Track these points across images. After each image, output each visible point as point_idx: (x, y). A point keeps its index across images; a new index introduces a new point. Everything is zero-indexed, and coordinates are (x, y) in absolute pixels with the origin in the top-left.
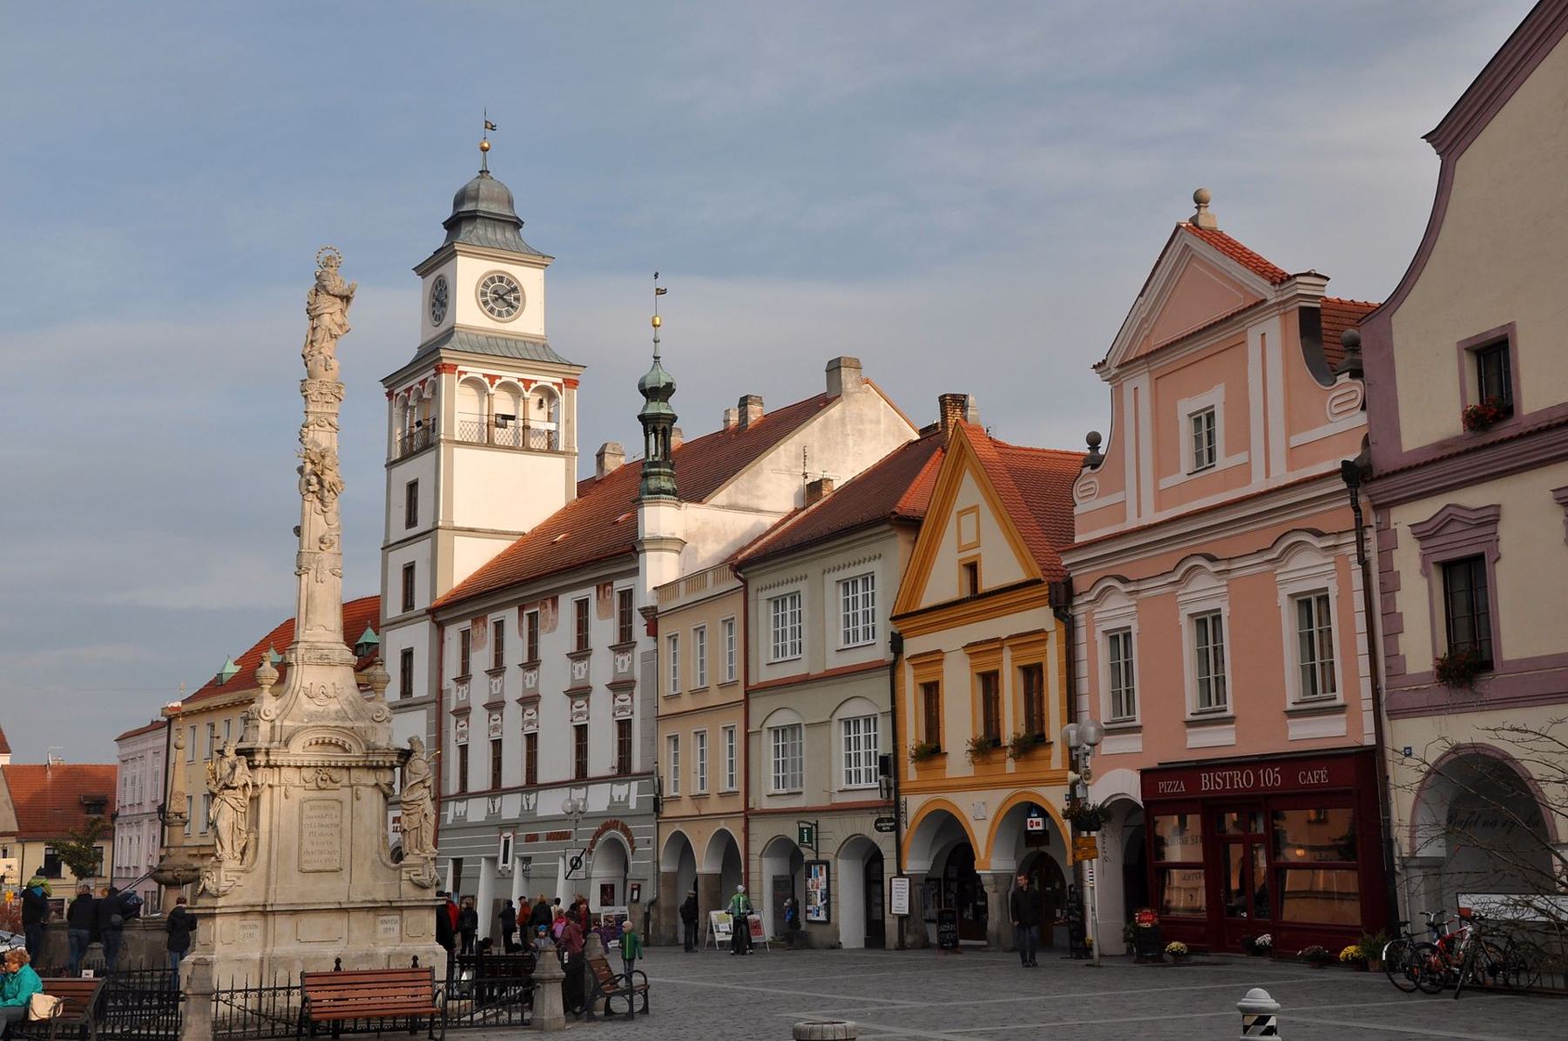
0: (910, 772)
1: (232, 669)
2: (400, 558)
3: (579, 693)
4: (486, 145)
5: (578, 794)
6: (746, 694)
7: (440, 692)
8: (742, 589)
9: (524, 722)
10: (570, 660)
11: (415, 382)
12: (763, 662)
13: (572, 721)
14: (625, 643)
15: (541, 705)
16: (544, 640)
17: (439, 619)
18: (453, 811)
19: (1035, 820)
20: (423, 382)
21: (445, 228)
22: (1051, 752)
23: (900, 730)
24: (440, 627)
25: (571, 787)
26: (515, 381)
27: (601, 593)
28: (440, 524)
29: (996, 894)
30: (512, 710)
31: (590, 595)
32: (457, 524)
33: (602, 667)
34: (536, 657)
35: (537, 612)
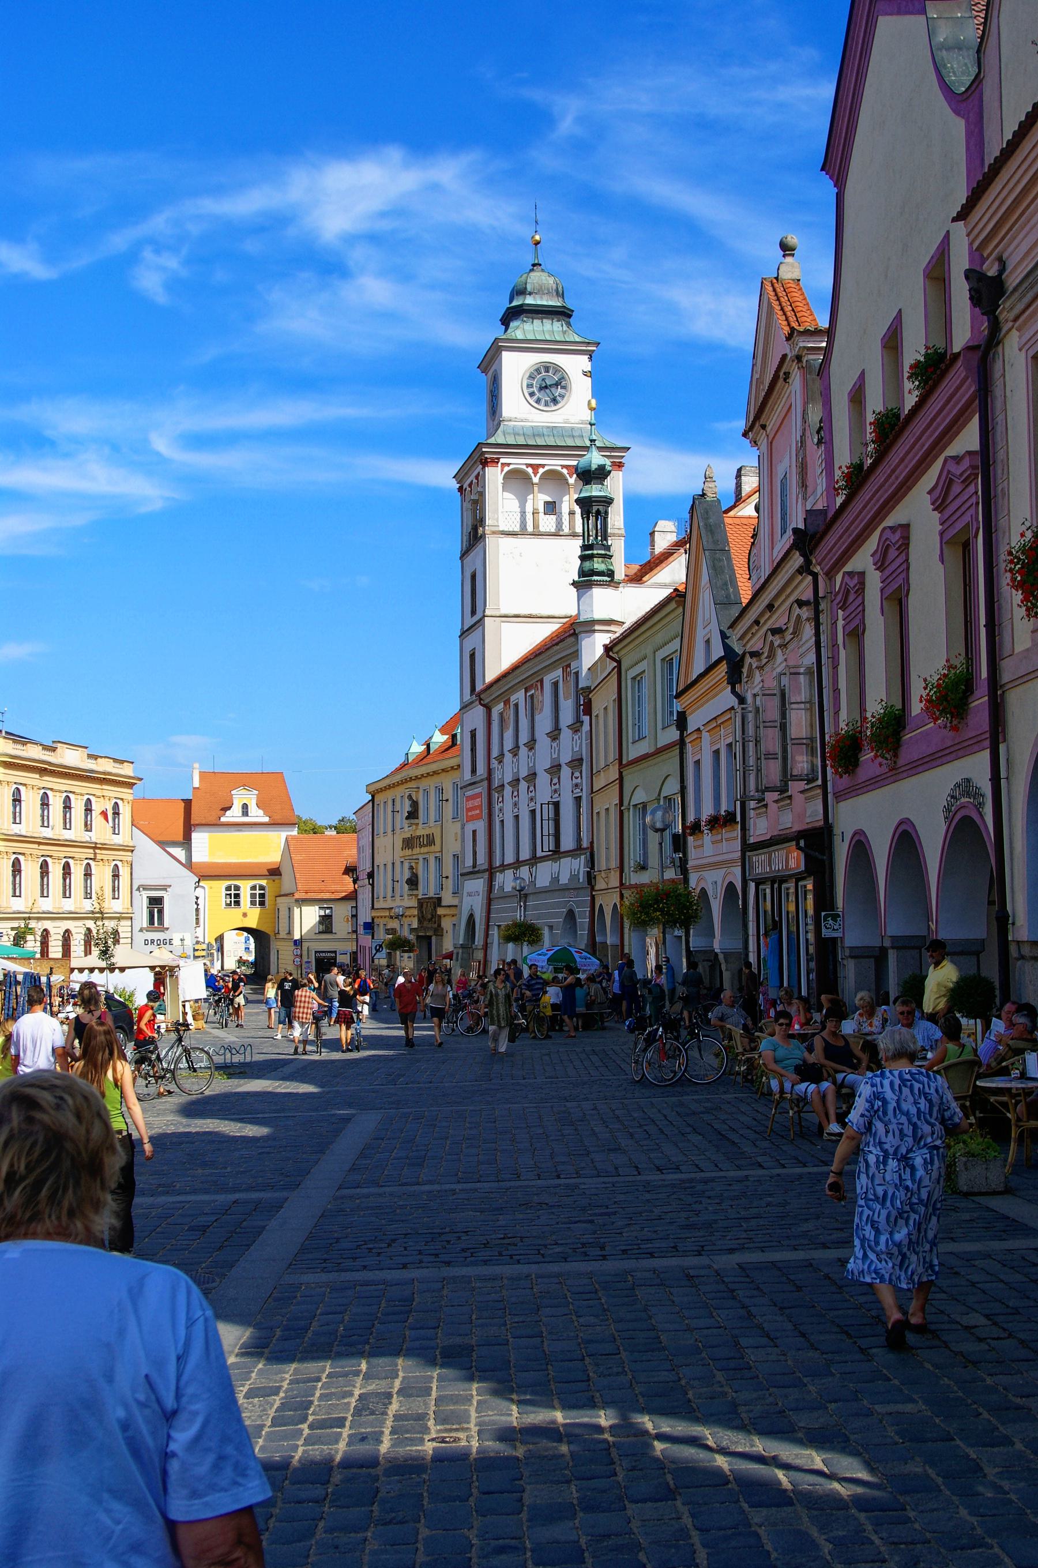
1: (417, 748)
2: (470, 642)
3: (555, 769)
4: (537, 238)
5: (556, 865)
6: (621, 773)
7: (490, 771)
11: (472, 477)
12: (630, 741)
14: (576, 726)
16: (537, 718)
17: (486, 702)
18: (499, 877)
20: (477, 477)
21: (502, 324)
24: (488, 709)
26: (559, 468)
28: (487, 613)
29: (729, 973)
30: (523, 785)
32: (503, 612)
33: (569, 746)
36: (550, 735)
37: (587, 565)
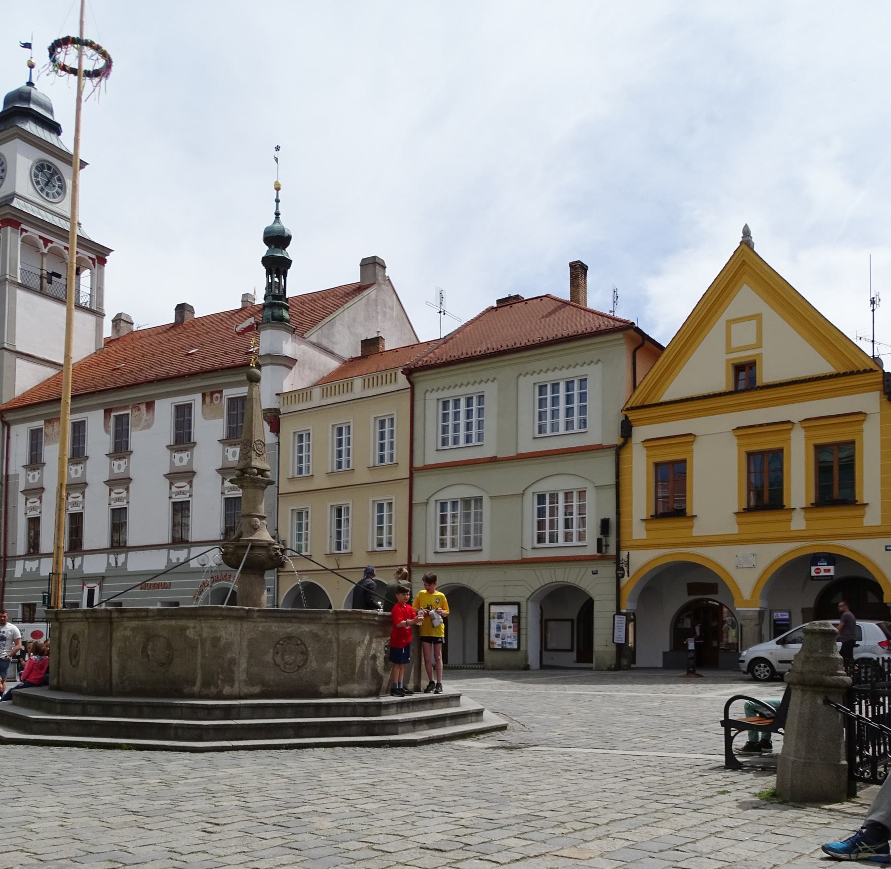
0: (637, 530)
5: (179, 555)
8: (410, 390)
9: (110, 499)
10: (169, 451)
13: (170, 498)
15: (131, 486)
17: (7, 419)
19: (822, 568)
22: (865, 513)
23: (623, 499)
25: (169, 549)
27: (208, 399)
31: (194, 400)
32: (18, 349)
34: (127, 449)
35: (128, 414)
36: (171, 447)
37: (277, 312)
